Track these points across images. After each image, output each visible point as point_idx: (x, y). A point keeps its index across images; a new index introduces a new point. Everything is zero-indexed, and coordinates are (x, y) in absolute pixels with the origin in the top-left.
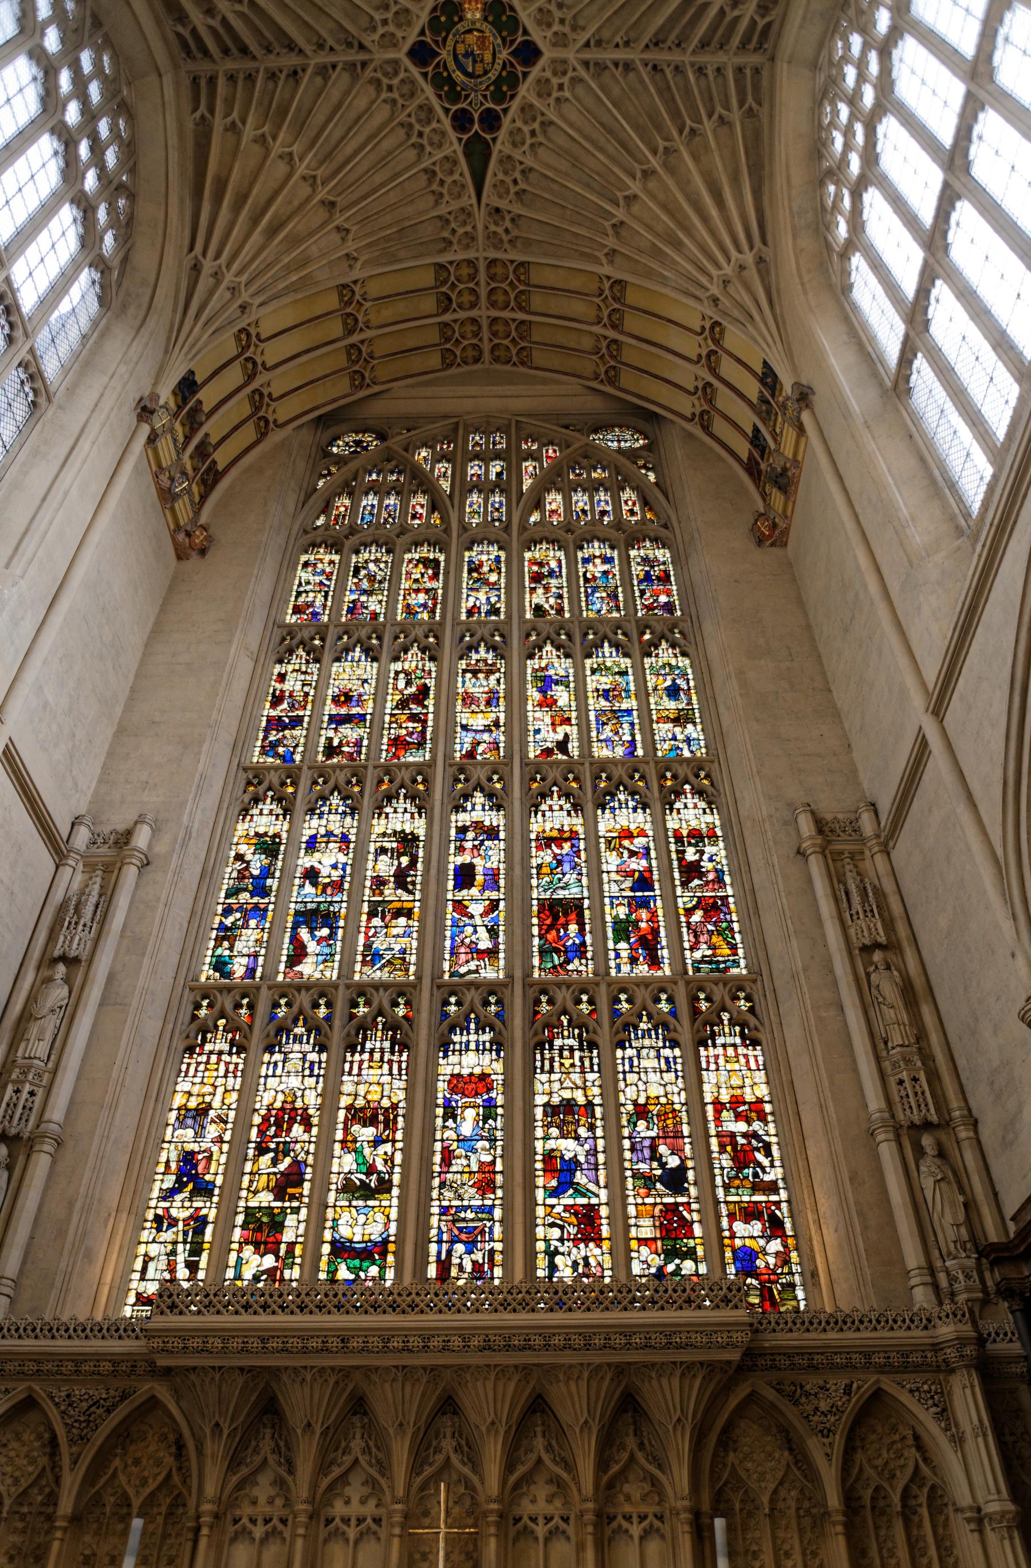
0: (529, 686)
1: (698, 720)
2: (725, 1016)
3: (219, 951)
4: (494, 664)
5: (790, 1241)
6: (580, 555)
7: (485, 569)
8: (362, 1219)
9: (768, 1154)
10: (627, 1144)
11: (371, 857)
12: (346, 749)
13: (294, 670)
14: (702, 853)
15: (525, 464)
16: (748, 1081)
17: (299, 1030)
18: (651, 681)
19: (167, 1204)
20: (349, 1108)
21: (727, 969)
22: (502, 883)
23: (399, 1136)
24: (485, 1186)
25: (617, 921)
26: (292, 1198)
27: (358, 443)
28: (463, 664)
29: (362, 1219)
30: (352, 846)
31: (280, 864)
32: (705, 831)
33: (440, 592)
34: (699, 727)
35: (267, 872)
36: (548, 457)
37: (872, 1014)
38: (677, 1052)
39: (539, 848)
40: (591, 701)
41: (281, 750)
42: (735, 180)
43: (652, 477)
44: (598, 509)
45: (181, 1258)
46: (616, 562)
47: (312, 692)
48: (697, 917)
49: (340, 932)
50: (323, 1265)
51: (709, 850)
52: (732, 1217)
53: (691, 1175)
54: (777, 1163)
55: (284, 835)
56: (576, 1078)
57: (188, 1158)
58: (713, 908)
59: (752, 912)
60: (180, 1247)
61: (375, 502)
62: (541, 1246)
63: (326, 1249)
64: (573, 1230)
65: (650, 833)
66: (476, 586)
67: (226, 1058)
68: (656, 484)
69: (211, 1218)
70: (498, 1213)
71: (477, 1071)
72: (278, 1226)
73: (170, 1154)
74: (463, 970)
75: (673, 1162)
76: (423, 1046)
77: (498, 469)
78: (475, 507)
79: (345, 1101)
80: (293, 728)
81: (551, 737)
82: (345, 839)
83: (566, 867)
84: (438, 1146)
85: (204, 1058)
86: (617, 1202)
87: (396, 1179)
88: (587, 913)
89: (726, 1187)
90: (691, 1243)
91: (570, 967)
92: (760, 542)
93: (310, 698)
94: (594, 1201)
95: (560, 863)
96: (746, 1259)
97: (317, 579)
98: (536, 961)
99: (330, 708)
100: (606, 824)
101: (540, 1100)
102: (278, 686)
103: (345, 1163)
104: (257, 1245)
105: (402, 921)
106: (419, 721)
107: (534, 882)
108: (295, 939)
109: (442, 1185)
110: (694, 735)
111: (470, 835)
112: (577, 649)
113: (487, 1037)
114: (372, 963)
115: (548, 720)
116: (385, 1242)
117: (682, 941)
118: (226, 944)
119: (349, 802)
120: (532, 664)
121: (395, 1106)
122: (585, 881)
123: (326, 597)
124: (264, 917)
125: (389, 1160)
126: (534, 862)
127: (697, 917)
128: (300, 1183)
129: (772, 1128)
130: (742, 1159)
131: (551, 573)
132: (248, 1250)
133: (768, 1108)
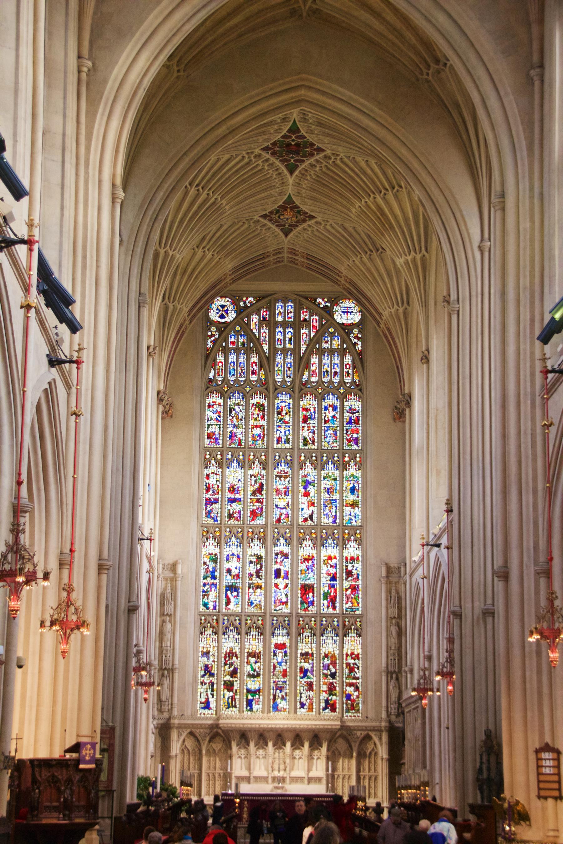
2: (353, 627)
4: (287, 473)
6: (324, 404)
7: (284, 413)
9: (358, 668)
11: (248, 565)
12: (235, 515)
13: (212, 473)
14: (353, 566)
17: (231, 628)
18: (346, 483)
19: (202, 679)
22: (289, 576)
25: (324, 593)
27: (223, 306)
32: (356, 557)
33: (266, 427)
35: (214, 570)
36: (313, 326)
39: (301, 563)
40: (322, 494)
41: (212, 515)
43: (359, 347)
44: (333, 371)
46: (338, 410)
48: (349, 592)
51: (356, 565)
52: (346, 686)
53: (337, 674)
55: (218, 554)
56: (309, 645)
58: (354, 589)
59: (365, 594)
61: (235, 360)
62: (298, 691)
63: (245, 691)
64: (306, 688)
65: (338, 558)
68: (360, 354)
70: (288, 683)
71: (282, 642)
73: (201, 665)
74: (278, 609)
75: (333, 670)
76: (267, 637)
77: (289, 336)
78: (279, 366)
80: (216, 503)
81: (306, 513)
82: (238, 557)
83: (310, 571)
84: (272, 664)
88: (315, 589)
92: (395, 420)
95: (308, 569)
96: (349, 697)
97: (215, 416)
98: (299, 606)
99: (228, 495)
100: (325, 553)
101: (299, 651)
102: (207, 481)
105: (259, 590)
107: (299, 576)
108: (227, 596)
110: (358, 513)
111: (279, 556)
112: (319, 467)
113: (285, 631)
114: (251, 605)
115: (306, 504)
120: (302, 473)
123: (220, 428)
124: (216, 587)
125: (259, 668)
126: (300, 568)
127: (349, 592)
128: (236, 673)
129: (360, 662)
130: (351, 670)
131: (311, 417)
132: (226, 691)
133: (360, 656)
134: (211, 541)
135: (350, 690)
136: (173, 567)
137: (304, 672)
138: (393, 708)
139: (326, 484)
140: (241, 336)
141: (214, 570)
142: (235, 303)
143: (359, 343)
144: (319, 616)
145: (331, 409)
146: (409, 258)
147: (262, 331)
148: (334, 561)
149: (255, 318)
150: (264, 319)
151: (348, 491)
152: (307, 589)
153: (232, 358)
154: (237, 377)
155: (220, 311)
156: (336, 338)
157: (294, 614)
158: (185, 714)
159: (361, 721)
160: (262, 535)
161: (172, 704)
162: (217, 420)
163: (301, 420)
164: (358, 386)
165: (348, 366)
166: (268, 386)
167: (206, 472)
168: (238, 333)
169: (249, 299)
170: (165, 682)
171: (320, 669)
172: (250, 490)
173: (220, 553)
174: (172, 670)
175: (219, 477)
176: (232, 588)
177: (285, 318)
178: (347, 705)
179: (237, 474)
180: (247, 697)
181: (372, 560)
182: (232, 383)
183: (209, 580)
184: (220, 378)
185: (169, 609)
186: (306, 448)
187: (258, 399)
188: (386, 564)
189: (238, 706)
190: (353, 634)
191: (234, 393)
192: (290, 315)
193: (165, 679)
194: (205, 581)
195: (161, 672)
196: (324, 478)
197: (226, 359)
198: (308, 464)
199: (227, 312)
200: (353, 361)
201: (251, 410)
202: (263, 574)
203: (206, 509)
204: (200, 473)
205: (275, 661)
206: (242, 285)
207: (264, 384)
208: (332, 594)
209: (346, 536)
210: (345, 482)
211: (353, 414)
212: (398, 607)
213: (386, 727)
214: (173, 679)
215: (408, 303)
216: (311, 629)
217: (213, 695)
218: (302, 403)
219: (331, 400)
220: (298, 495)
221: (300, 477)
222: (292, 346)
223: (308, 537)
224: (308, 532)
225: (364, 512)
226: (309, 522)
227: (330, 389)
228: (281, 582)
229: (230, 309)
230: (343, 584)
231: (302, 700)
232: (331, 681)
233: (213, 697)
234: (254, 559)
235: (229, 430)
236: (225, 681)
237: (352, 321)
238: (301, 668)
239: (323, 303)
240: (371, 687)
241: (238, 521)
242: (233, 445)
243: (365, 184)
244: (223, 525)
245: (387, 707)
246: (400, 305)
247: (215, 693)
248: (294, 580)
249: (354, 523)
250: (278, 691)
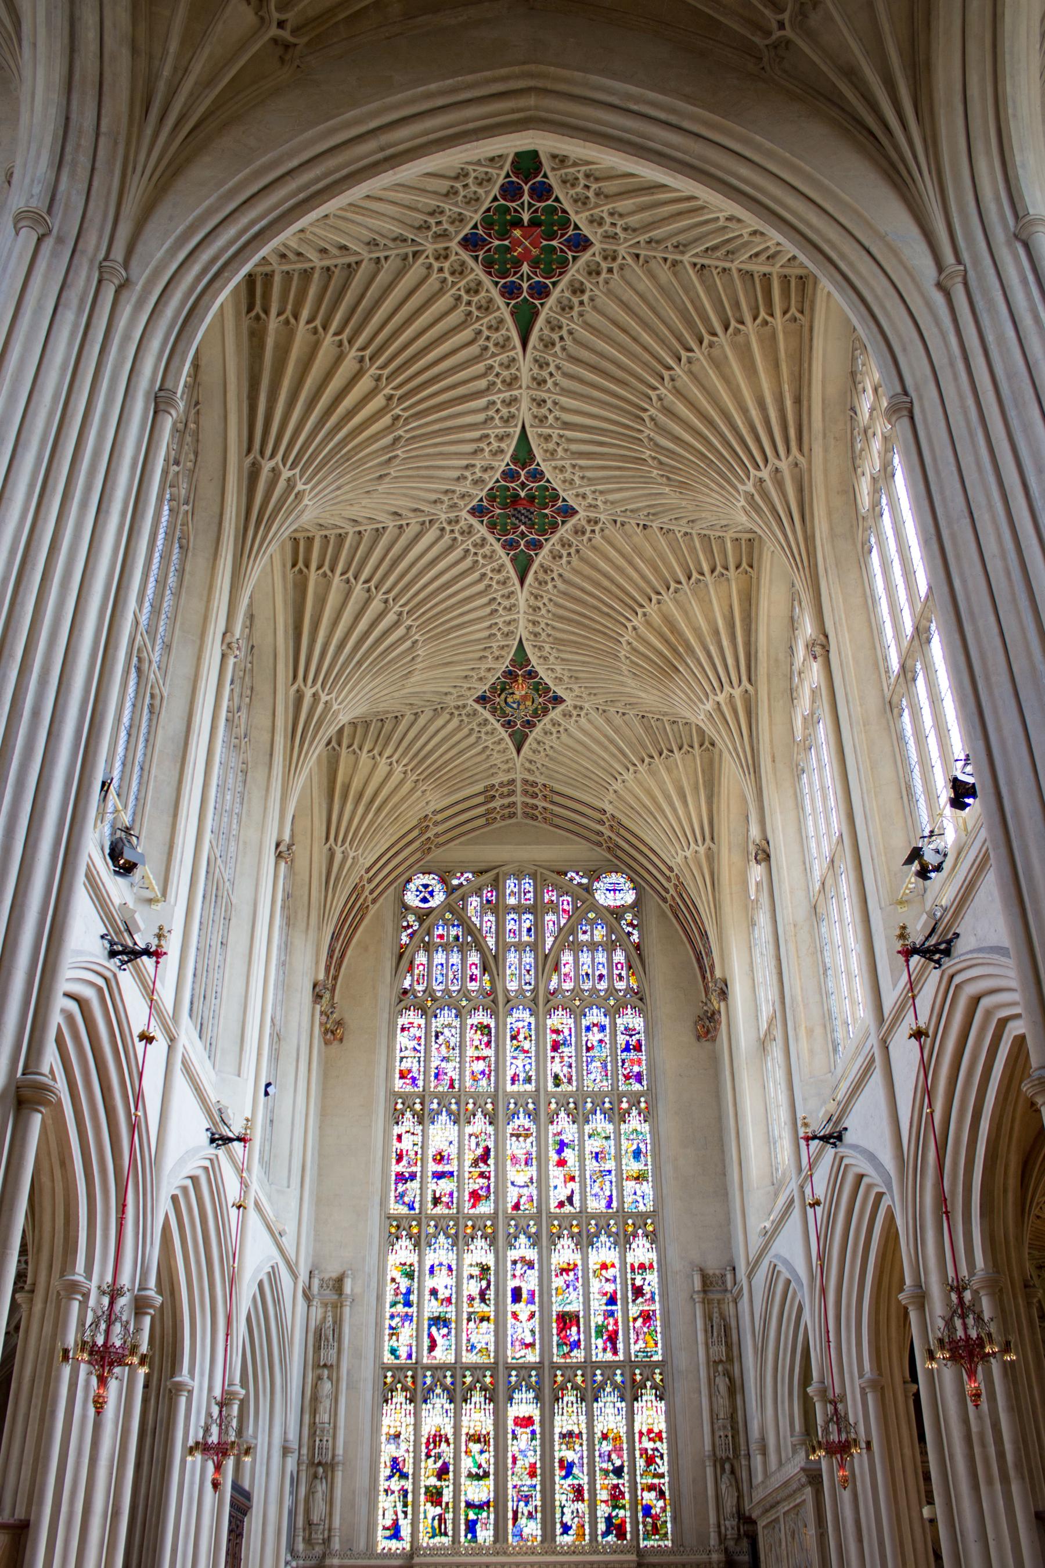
0: (550, 1149)
1: (650, 1179)
2: (649, 1384)
3: (391, 1343)
4: (528, 1130)
5: (668, 1502)
6: (583, 1021)
7: (521, 1037)
8: (477, 1490)
9: (662, 1457)
10: (597, 1453)
14: (644, 1279)
15: (547, 918)
16: (656, 1421)
17: (438, 1391)
18: (625, 1144)
19: (387, 1483)
20: (467, 1434)
21: (651, 1356)
22: (537, 1299)
23: (492, 1448)
24: (532, 1474)
26: (445, 1480)
27: (426, 886)
28: (509, 1129)
29: (477, 1490)
30: (454, 1273)
31: (416, 1285)
32: (647, 1265)
34: (650, 1184)
35: (409, 1292)
36: (564, 911)
37: (714, 1399)
38: (624, 1404)
39: (557, 1276)
40: (587, 1162)
42: (696, 788)
43: (635, 938)
44: (597, 973)
45: (400, 1508)
47: (420, 1152)
48: (639, 1323)
49: (453, 1331)
50: (462, 1512)
52: (643, 1490)
53: (626, 1469)
54: (666, 1463)
56: (574, 1418)
57: (395, 1460)
60: (398, 1504)
61: (444, 961)
62: (557, 1503)
63: (463, 1505)
64: (571, 1496)
65: (617, 1265)
66: (515, 1054)
67: (404, 1406)
68: (638, 947)
69: (410, 1490)
71: (527, 1415)
72: (439, 1493)
73: (385, 1458)
74: (518, 1355)
75: (618, 1463)
77: (527, 924)
78: (513, 968)
79: (464, 1431)
80: (412, 1180)
81: (562, 1194)
82: (450, 1268)
83: (571, 1288)
85: (393, 1407)
86: (592, 1482)
87: (492, 1471)
88: (582, 1320)
89: (641, 1475)
90: (624, 1502)
91: (572, 1354)
92: (699, 1038)
93: (419, 1156)
94: (581, 1482)
95: (568, 1286)
96: (647, 1510)
98: (555, 1350)
99: (433, 1167)
100: (596, 1258)
103: (467, 1464)
104: (432, 1503)
105: (485, 1323)
106: (485, 1177)
107: (554, 1299)
108: (430, 1336)
109: (513, 1474)
110: (647, 1191)
111: (519, 1265)
112: (581, 1119)
113: (532, 1395)
114: (471, 1350)
115: (562, 1179)
116: (489, 1501)
117: (629, 1338)
118: (394, 1338)
119: (450, 1240)
120: (553, 1129)
121: (488, 1434)
122: (581, 1299)
123: (419, 1062)
124: (411, 1320)
126: (554, 1286)
128: (447, 1473)
129: (665, 1446)
130: (650, 1460)
132: (429, 1504)
133: (664, 1435)
134: (404, 1242)
135: (649, 1497)
136: (338, 1284)
137: (568, 1468)
138: (730, 1523)
139: (592, 1145)
140: (454, 926)
141: (409, 1292)
142: (443, 881)
143: (635, 932)
144: (589, 1366)
145: (595, 1029)
146: (721, 698)
147: (486, 919)
148: (610, 1273)
149: (474, 902)
150: (488, 901)
151: (630, 1155)
152: (566, 1320)
153: (439, 958)
154: (447, 985)
155: (421, 892)
156: (599, 927)
157: (546, 1363)
158: (354, 1549)
159: (671, 1552)
160: (489, 1231)
161: (330, 1530)
162: (415, 1049)
163: (549, 1047)
164: (636, 993)
165: (619, 966)
166: (496, 997)
167: (397, 1130)
168: (446, 923)
169: (466, 875)
170: (319, 1488)
171: (595, 1462)
172: (469, 1157)
173: (419, 1262)
174: (330, 1467)
175: (418, 1139)
176: (438, 1321)
177: (520, 901)
178: (645, 1526)
179: (447, 1134)
180: (467, 1515)
181: (676, 1264)
182: (439, 994)
183: (400, 1308)
184: (420, 988)
185: (329, 1355)
186: (559, 1089)
187: (481, 1017)
188: (701, 1270)
189: (450, 1533)
190: (649, 1395)
191: (442, 1009)
192: (528, 896)
193: (318, 1481)
194: (393, 1310)
195: (312, 1470)
196: (590, 1137)
197: (430, 960)
198: (562, 1114)
199: (431, 893)
200: (627, 958)
201: (470, 1034)
202: (492, 1297)
203: (396, 1189)
204: (387, 1132)
205: (515, 1448)
206: (455, 852)
207: (489, 995)
208: (610, 1328)
209: (630, 1229)
210: (623, 1141)
211: (631, 1036)
212: (726, 1342)
213: (719, 1562)
214: (332, 1483)
215: (712, 839)
216: (576, 1389)
217: (405, 1513)
218: (549, 1022)
219: (595, 1016)
220: (547, 1164)
221: (551, 1135)
222: (532, 939)
223: (565, 1232)
224: (566, 1224)
225: (657, 1188)
226: (568, 1209)
227: (594, 1000)
228: (523, 1309)
229: (436, 889)
230: (628, 1310)
231: (565, 1520)
232: (615, 1482)
233: (406, 1517)
234: (476, 1271)
235: (434, 1065)
236: (427, 1487)
237: (623, 902)
238: (561, 1461)
239: (577, 878)
240: (687, 1489)
241: (449, 1208)
242: (440, 1089)
243: (643, 577)
244: (423, 1215)
245: (719, 1526)
246: (700, 842)
247: (409, 1509)
248: (545, 1305)
249: (642, 1208)
250: (522, 1504)
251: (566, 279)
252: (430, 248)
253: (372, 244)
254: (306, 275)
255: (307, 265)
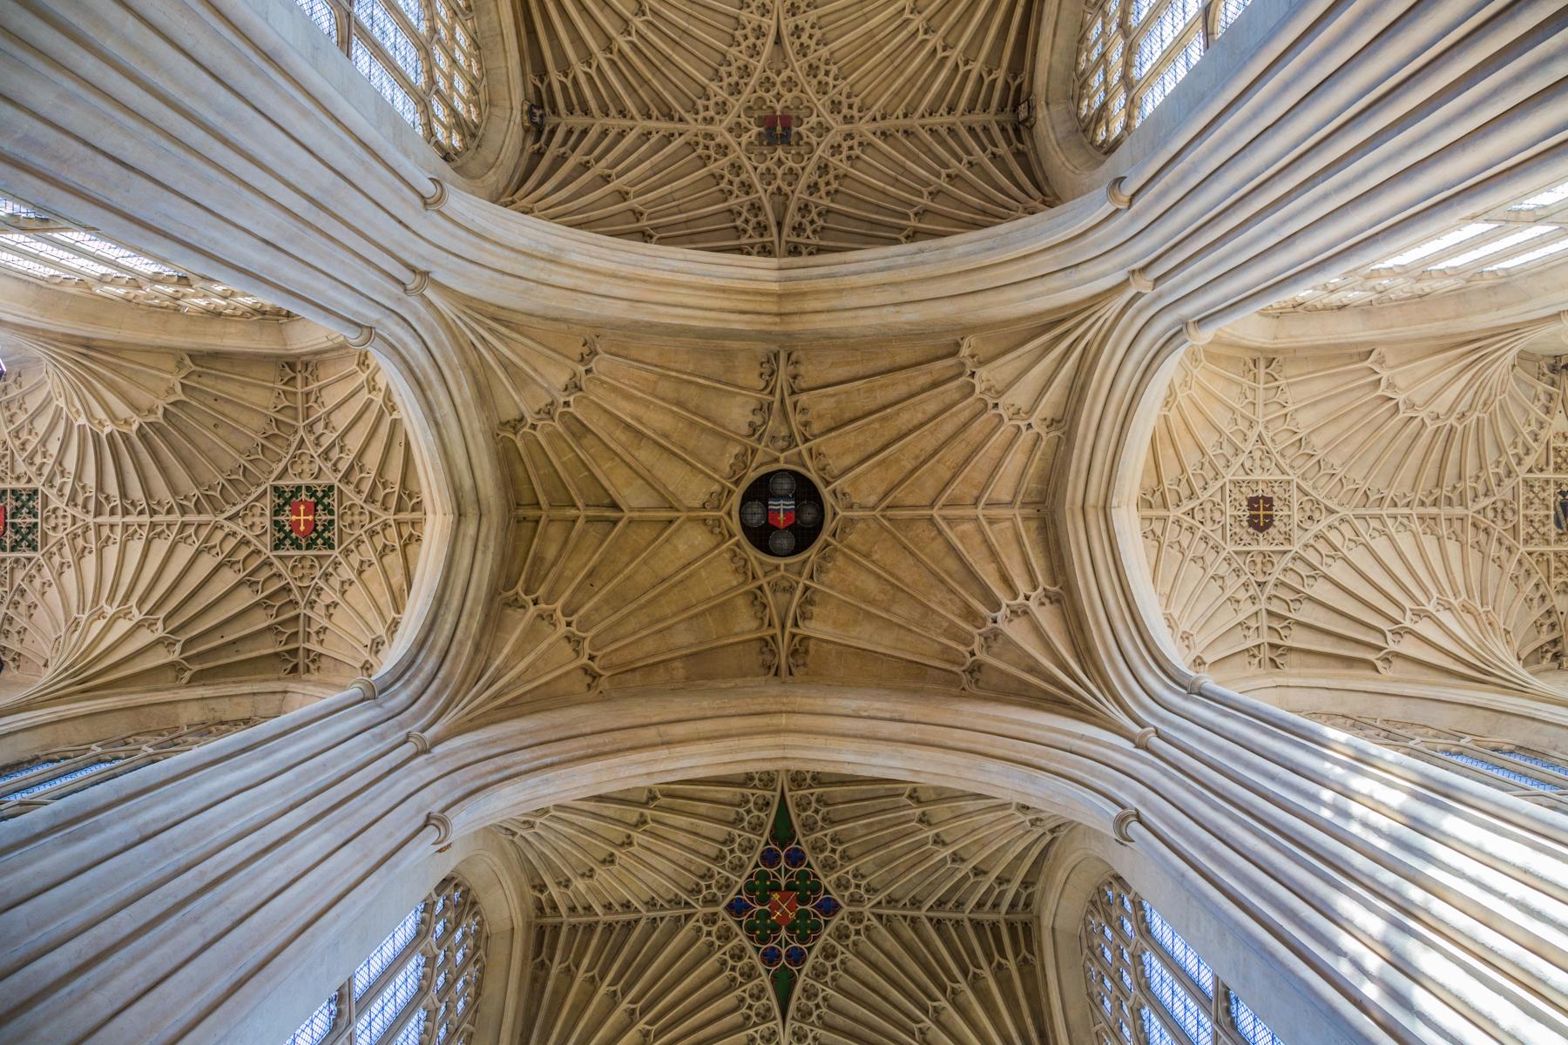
251: (819, 944)
252: (701, 910)
253: (651, 904)
254: (590, 928)
255: (592, 919)
